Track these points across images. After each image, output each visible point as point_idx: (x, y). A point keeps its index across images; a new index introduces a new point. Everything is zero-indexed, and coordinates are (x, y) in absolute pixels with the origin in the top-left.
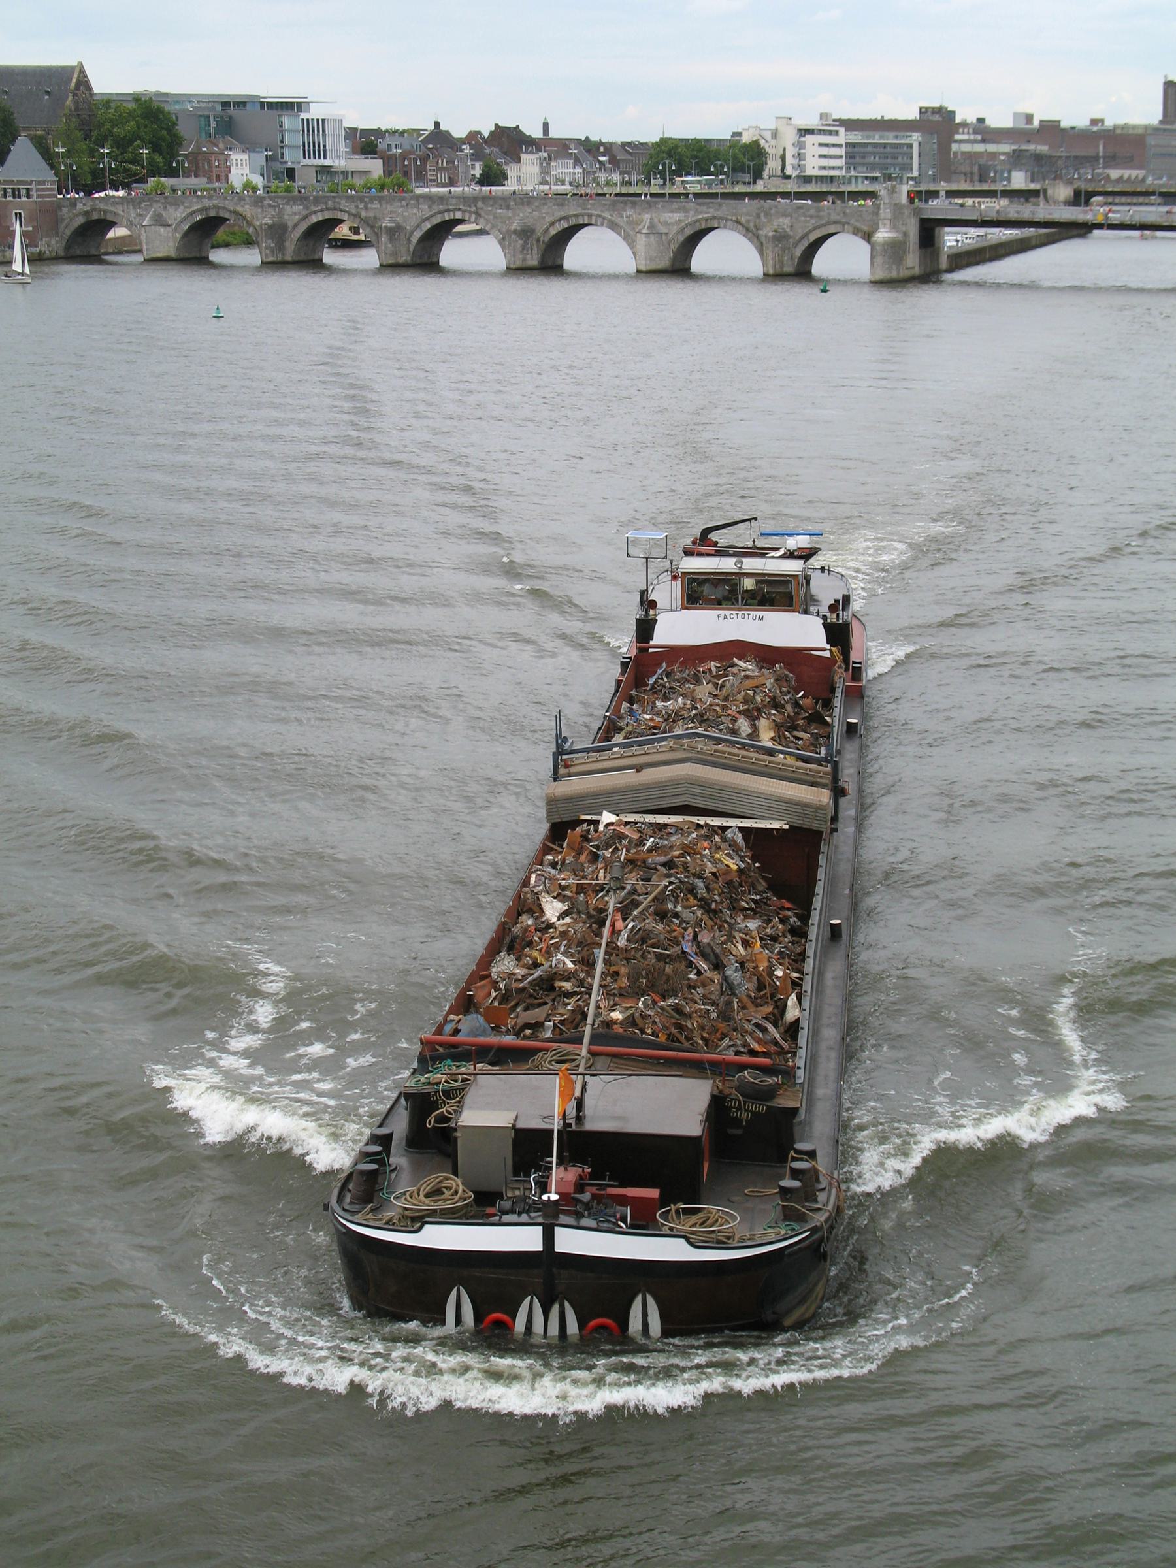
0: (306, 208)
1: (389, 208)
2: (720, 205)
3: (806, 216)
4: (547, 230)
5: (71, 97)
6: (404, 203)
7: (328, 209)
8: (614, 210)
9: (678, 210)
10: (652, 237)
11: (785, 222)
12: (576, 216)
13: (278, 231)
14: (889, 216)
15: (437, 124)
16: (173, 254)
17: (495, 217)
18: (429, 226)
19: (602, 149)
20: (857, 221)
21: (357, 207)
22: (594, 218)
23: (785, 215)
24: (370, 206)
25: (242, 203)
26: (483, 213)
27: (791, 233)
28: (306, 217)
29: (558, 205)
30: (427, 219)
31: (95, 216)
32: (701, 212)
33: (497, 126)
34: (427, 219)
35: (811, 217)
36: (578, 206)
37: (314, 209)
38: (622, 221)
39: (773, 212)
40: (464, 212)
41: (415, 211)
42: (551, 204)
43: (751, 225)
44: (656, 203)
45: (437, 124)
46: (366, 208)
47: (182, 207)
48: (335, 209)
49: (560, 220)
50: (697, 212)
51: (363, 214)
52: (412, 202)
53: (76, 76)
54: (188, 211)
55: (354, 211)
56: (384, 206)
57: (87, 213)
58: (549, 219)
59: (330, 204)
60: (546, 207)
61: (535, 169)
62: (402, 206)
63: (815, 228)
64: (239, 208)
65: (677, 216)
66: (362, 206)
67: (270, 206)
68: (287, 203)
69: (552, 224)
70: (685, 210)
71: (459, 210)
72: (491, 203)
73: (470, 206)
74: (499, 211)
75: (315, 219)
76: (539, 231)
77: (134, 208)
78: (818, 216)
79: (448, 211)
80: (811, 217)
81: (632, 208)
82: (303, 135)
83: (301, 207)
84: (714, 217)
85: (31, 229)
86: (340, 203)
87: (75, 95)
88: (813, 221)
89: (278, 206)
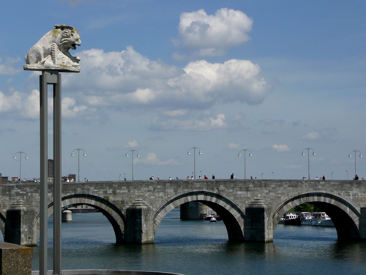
1: (137, 192)
6: (151, 188)
7: (76, 196)
8: (342, 190)
24: (118, 191)
29: (292, 186)
34: (172, 201)
36: (310, 187)
41: (161, 194)
42: (287, 186)
46: (114, 193)
49: (292, 200)
52: (159, 187)
56: (132, 191)
58: (284, 199)
59: (79, 191)
60: (282, 188)
66: (110, 191)
67: (18, 194)
69: (286, 203)
72: (232, 186)
73: (213, 189)
74: (239, 193)
81: (357, 187)
86: (89, 190)
89: (27, 195)
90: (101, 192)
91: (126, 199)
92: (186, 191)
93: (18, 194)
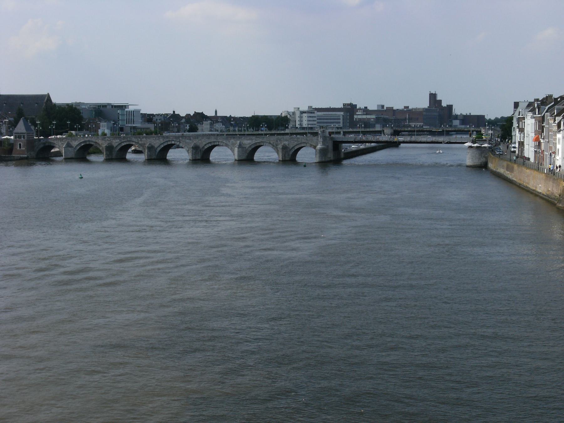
0: (120, 141)
1: (149, 140)
2: (264, 138)
3: (293, 141)
4: (203, 147)
5: (44, 105)
6: (154, 138)
7: (128, 141)
9: (249, 139)
10: (240, 149)
11: (286, 143)
12: (214, 142)
13: (110, 148)
14: (322, 140)
15: (174, 112)
16: (74, 156)
17: (186, 143)
18: (163, 146)
19: (232, 119)
20: (311, 142)
21: (138, 140)
22: (220, 143)
23: (286, 140)
25: (98, 139)
26: (181, 141)
27: (289, 147)
28: (120, 144)
30: (162, 144)
31: (47, 144)
32: (257, 140)
33: (195, 112)
35: (295, 141)
37: (123, 141)
38: (229, 144)
39: (282, 140)
40: (175, 141)
41: (158, 141)
42: (205, 138)
43: (275, 144)
44: (242, 137)
45: (174, 112)
47: (77, 141)
48: (130, 141)
49: (208, 144)
50: (256, 140)
51: (140, 142)
52: (157, 138)
53: (47, 98)
54: (79, 142)
55: (137, 141)
57: (44, 143)
58: (204, 143)
59: (129, 139)
61: (209, 126)
62: (154, 140)
63: (296, 145)
64: (97, 141)
65: (249, 142)
66: (139, 140)
67: (108, 140)
68: (114, 139)
70: (252, 140)
71: (173, 140)
74: (187, 141)
75: (123, 144)
76: (201, 147)
77: (61, 141)
78: (297, 141)
79: (169, 141)
80: (295, 141)
82: (126, 116)
83: (118, 140)
84: (262, 142)
85: (24, 149)
87: (46, 104)
88: (296, 142)
90: (136, 140)
91: (145, 143)
92: (167, 140)
93: (108, 140)
